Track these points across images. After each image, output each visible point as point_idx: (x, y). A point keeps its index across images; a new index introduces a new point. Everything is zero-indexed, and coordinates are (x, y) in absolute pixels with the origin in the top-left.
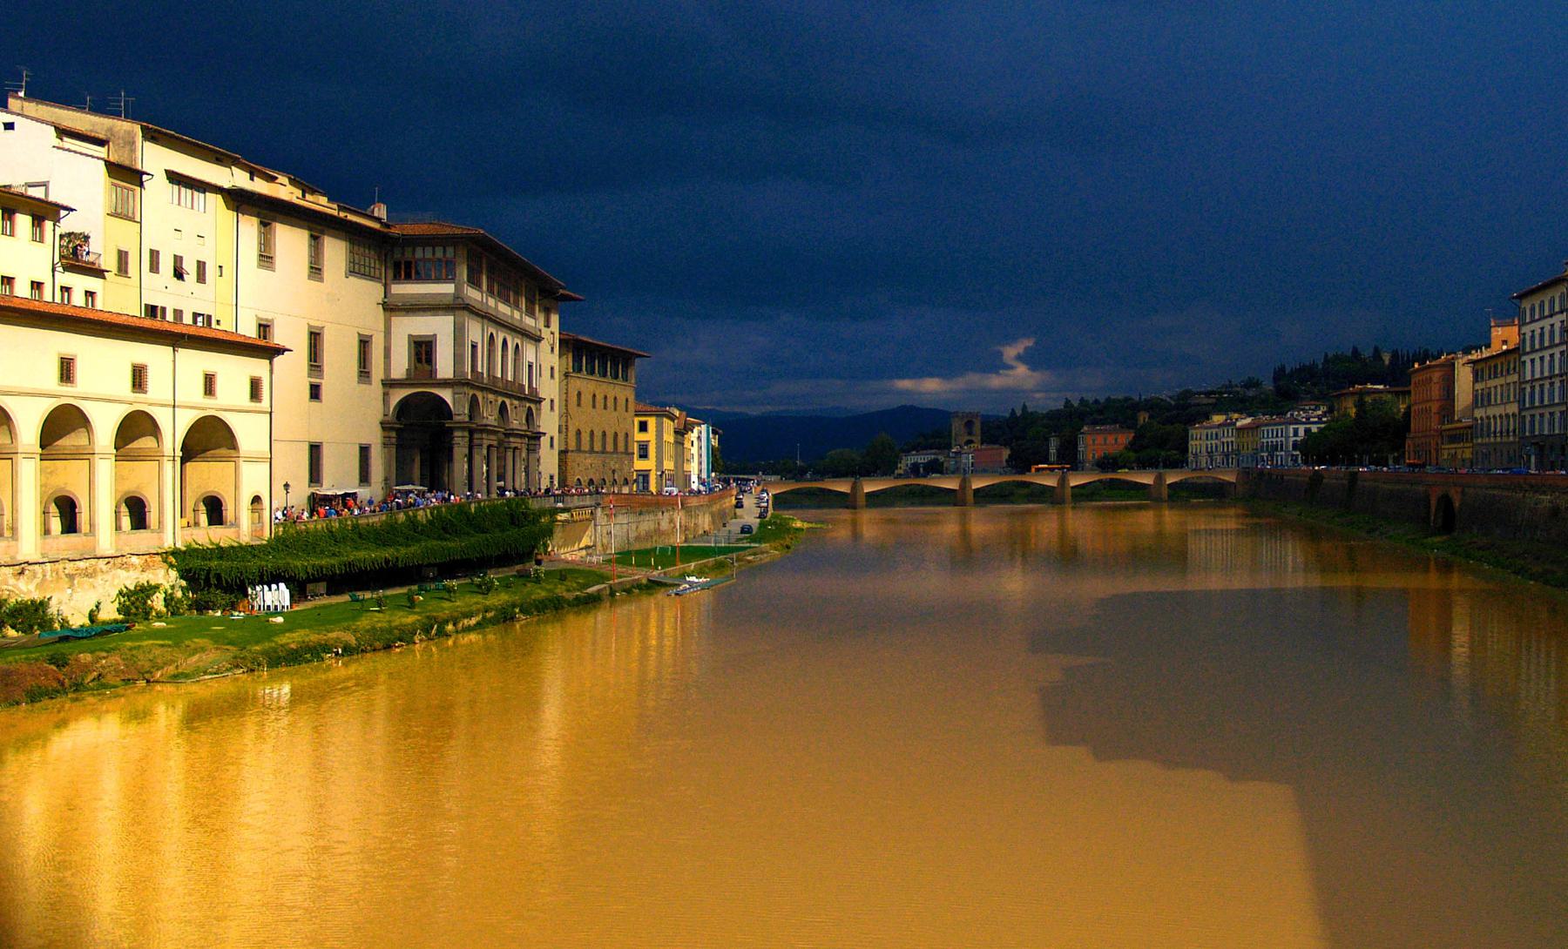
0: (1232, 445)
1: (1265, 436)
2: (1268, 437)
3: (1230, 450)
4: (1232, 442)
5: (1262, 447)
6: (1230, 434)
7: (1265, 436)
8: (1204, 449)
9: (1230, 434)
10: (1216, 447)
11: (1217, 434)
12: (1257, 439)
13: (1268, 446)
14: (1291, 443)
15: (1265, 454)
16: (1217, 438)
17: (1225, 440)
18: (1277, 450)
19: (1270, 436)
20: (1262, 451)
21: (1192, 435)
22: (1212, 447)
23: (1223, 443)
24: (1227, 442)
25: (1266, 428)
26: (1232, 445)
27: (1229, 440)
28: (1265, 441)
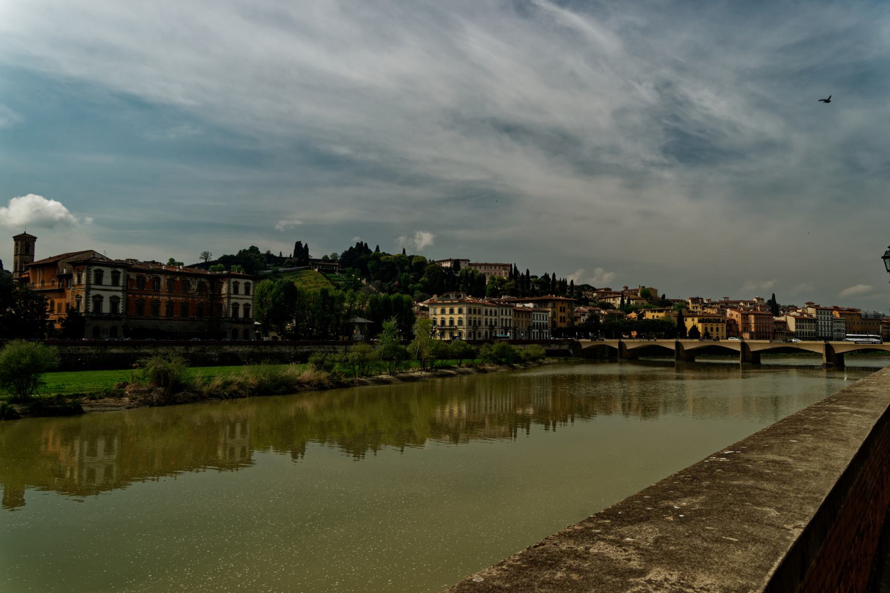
1: (535, 318)
3: (508, 325)
5: (534, 325)
6: (508, 313)
7: (535, 318)
8: (483, 323)
9: (508, 313)
10: (496, 322)
11: (496, 312)
13: (537, 325)
15: (536, 331)
16: (496, 315)
17: (505, 317)
18: (544, 328)
20: (534, 328)
22: (491, 322)
24: (507, 319)
25: (535, 313)
27: (509, 318)
28: (536, 321)
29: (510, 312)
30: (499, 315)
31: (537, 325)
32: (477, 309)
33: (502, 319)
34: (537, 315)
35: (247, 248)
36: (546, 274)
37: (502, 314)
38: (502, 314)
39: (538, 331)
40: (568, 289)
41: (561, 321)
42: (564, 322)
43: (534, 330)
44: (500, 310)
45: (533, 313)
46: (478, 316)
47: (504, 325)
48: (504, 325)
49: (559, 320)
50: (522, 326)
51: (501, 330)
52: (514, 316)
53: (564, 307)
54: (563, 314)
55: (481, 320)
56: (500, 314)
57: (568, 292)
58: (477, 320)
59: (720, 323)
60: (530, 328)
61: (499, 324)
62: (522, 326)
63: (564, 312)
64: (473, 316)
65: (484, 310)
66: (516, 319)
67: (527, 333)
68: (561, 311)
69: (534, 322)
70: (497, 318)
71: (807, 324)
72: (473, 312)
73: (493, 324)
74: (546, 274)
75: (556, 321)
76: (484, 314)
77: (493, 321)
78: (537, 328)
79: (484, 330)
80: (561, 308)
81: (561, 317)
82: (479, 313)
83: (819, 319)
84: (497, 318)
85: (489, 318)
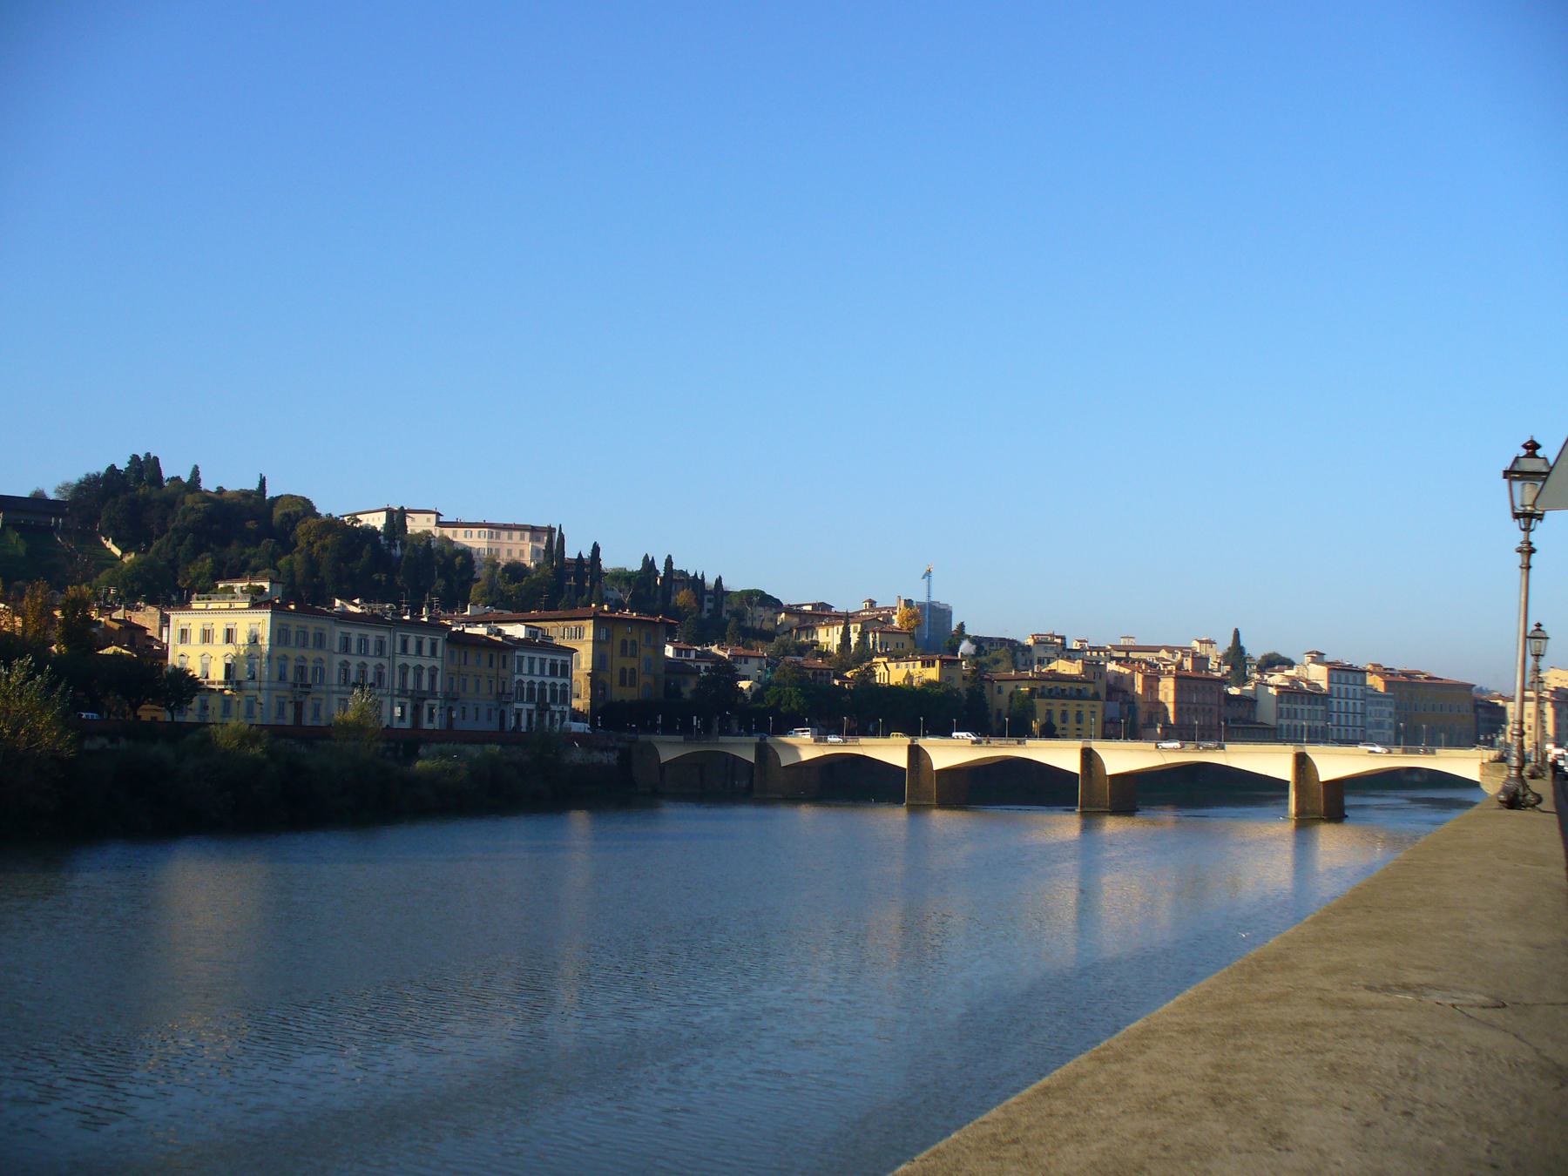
0: (433, 678)
1: (526, 670)
2: (531, 672)
3: (425, 686)
7: (526, 670)
10: (379, 675)
11: (381, 644)
13: (531, 690)
17: (412, 662)
19: (537, 670)
20: (521, 701)
25: (526, 655)
26: (433, 678)
27: (427, 663)
28: (526, 679)
31: (531, 690)
33: (405, 668)
34: (531, 660)
36: (646, 557)
38: (404, 649)
39: (532, 706)
40: (709, 600)
41: (623, 683)
42: (633, 685)
43: (517, 706)
44: (398, 639)
45: (517, 653)
46: (311, 655)
47: (410, 685)
48: (410, 685)
49: (617, 680)
51: (397, 700)
53: (634, 643)
54: (629, 664)
55: (325, 665)
56: (398, 650)
57: (709, 610)
58: (310, 665)
59: (1086, 698)
60: (503, 697)
64: (294, 653)
65: (337, 635)
67: (493, 713)
68: (623, 652)
69: (521, 682)
70: (384, 662)
71: (1306, 707)
72: (311, 640)
74: (646, 557)
75: (608, 682)
76: (337, 650)
77: (371, 671)
78: (531, 699)
79: (335, 697)
80: (624, 643)
81: (623, 670)
82: (320, 641)
83: (1335, 695)
84: (384, 662)
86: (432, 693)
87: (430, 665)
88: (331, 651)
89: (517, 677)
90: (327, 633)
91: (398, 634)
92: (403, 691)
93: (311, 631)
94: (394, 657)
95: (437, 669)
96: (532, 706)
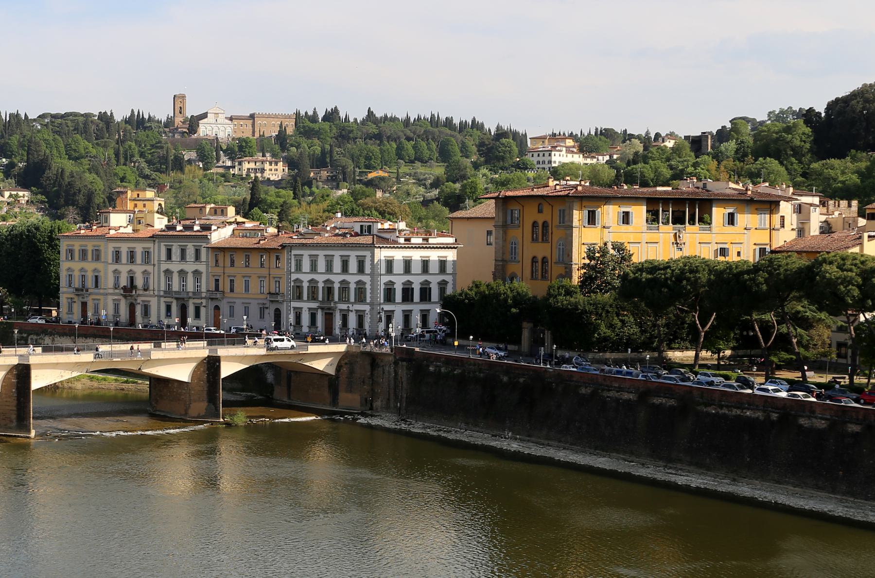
2: (314, 268)
4: (197, 273)
11: (147, 254)
12: (275, 272)
14: (383, 287)
15: (306, 306)
21: (71, 252)
23: (168, 272)
25: (306, 253)
27: (190, 267)
28: (305, 278)
29: (197, 252)
30: (159, 261)
32: (90, 249)
35: (401, 116)
37: (169, 257)
38: (169, 257)
39: (314, 305)
46: (90, 266)
48: (176, 287)
50: (247, 289)
51: (162, 300)
52: (212, 262)
53: (545, 225)
55: (102, 274)
56: (163, 256)
61: (158, 283)
62: (247, 289)
63: (545, 240)
66: (219, 270)
68: (534, 240)
73: (90, 283)
76: (110, 261)
78: (313, 296)
79: (110, 298)
80: (535, 224)
81: (534, 260)
82: (97, 257)
84: (149, 268)
85: (124, 269)
86: (197, 294)
87: (194, 269)
88: (106, 262)
89: (294, 277)
90: (102, 248)
91: (162, 244)
92: (168, 292)
93: (90, 249)
94: (159, 264)
95: (149, 274)
96: (314, 305)
